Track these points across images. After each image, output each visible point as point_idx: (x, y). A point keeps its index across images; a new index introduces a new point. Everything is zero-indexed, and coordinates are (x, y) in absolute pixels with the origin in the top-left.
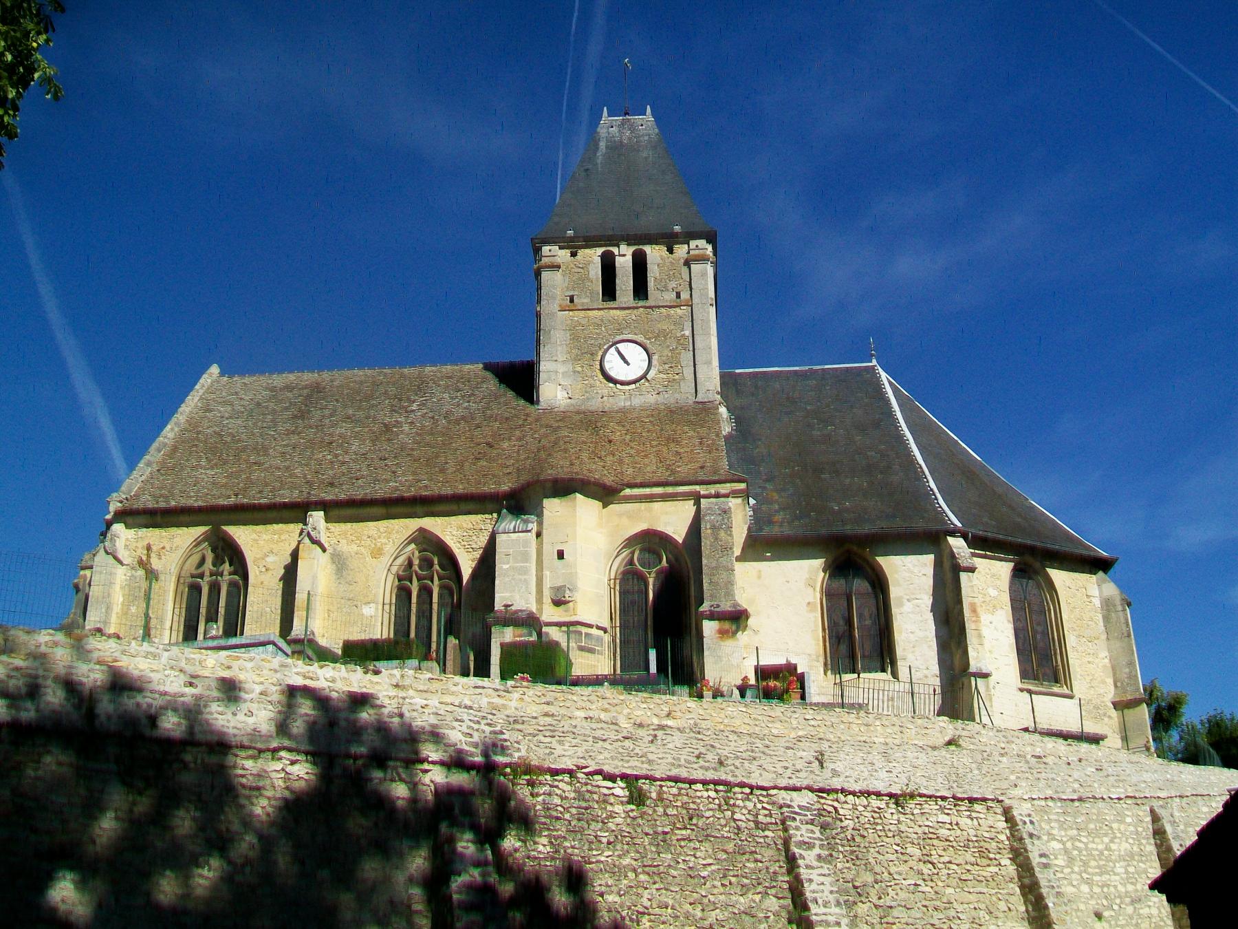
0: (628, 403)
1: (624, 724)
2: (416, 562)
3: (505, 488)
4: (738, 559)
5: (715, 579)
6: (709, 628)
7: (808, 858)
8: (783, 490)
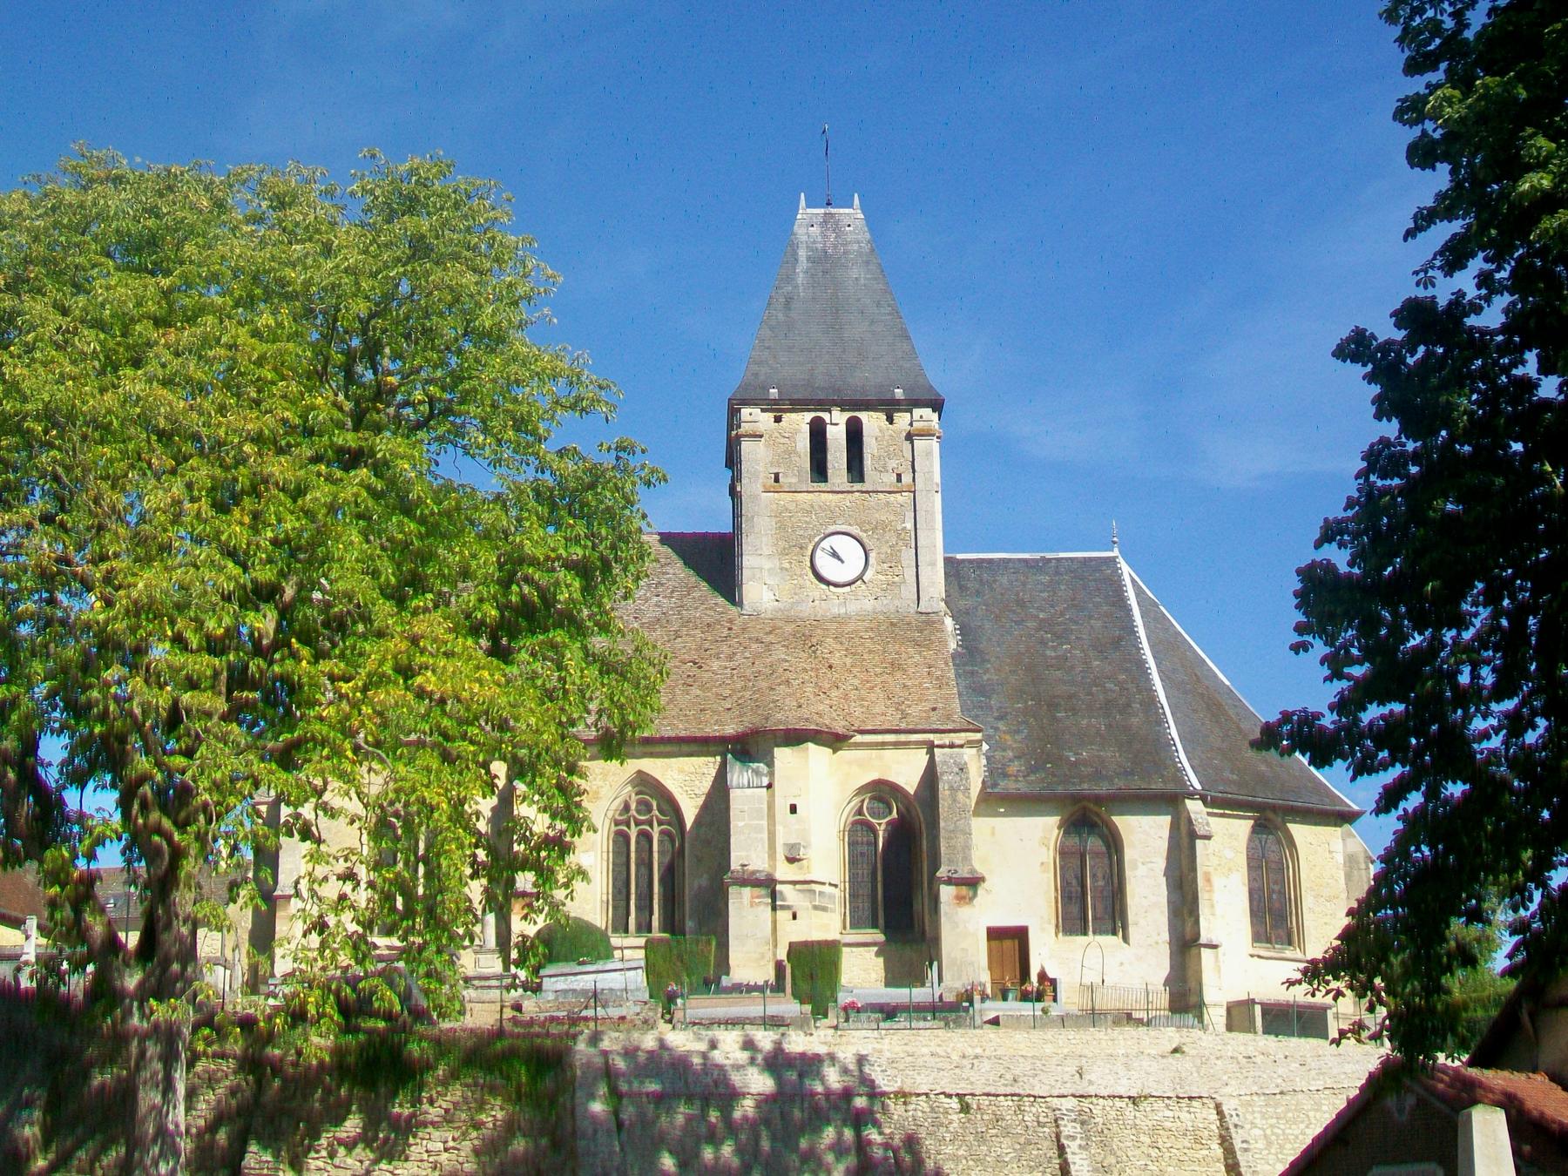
0: (843, 611)
1: (955, 1057)
2: (633, 806)
3: (730, 730)
5: (953, 842)
6: (946, 893)
7: (1072, 1147)
8: (1018, 732)
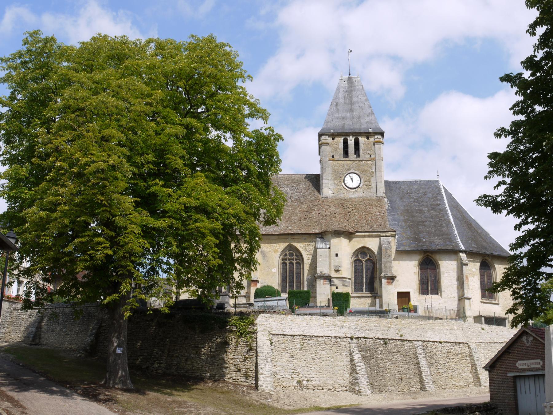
0: (353, 196)
4: (394, 260)
6: (384, 281)
7: (421, 357)
